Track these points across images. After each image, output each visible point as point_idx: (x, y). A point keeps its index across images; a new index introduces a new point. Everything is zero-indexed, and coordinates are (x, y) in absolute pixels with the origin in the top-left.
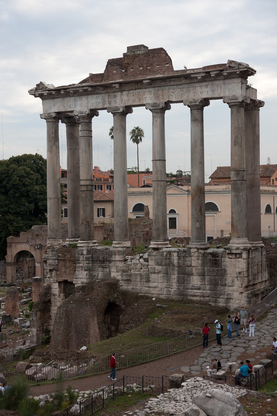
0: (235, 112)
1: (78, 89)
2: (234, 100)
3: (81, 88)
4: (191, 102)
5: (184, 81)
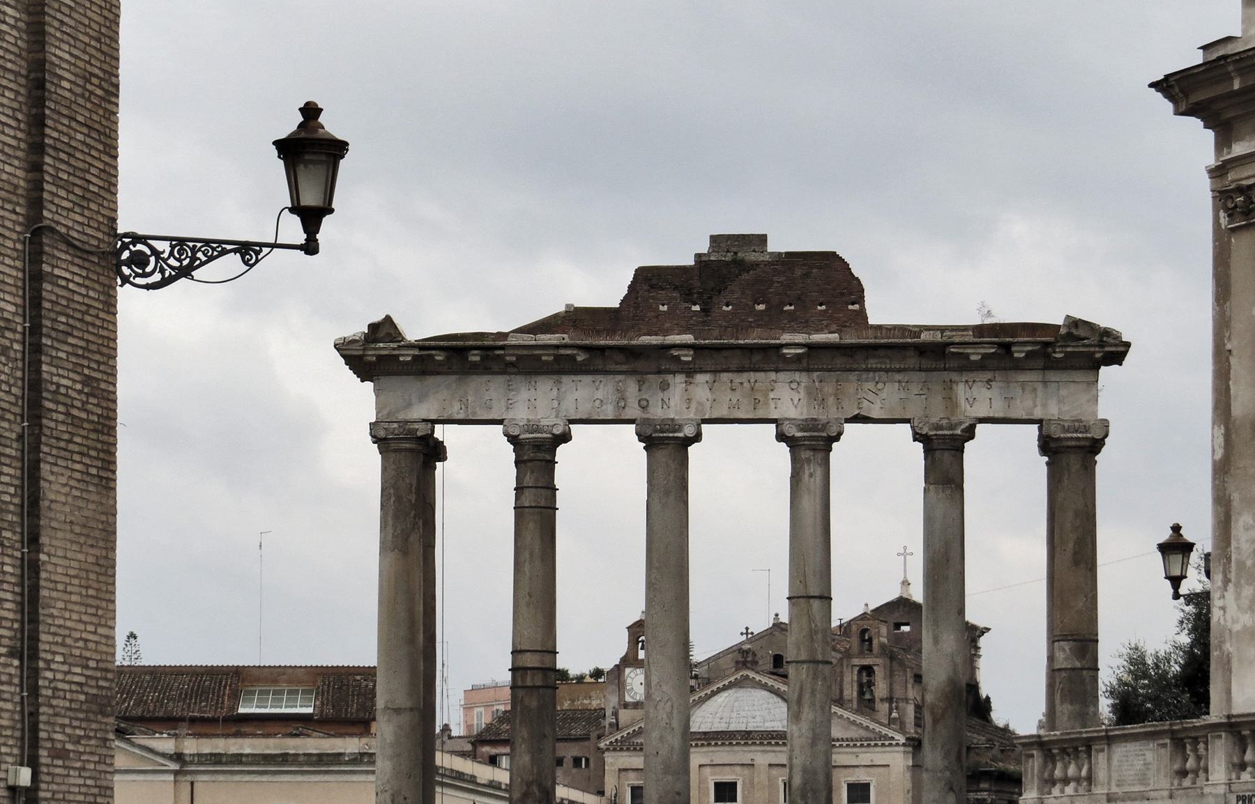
0: (1078, 466)
1: (538, 352)
2: (1076, 431)
3: (552, 352)
4: (938, 427)
5: (912, 361)
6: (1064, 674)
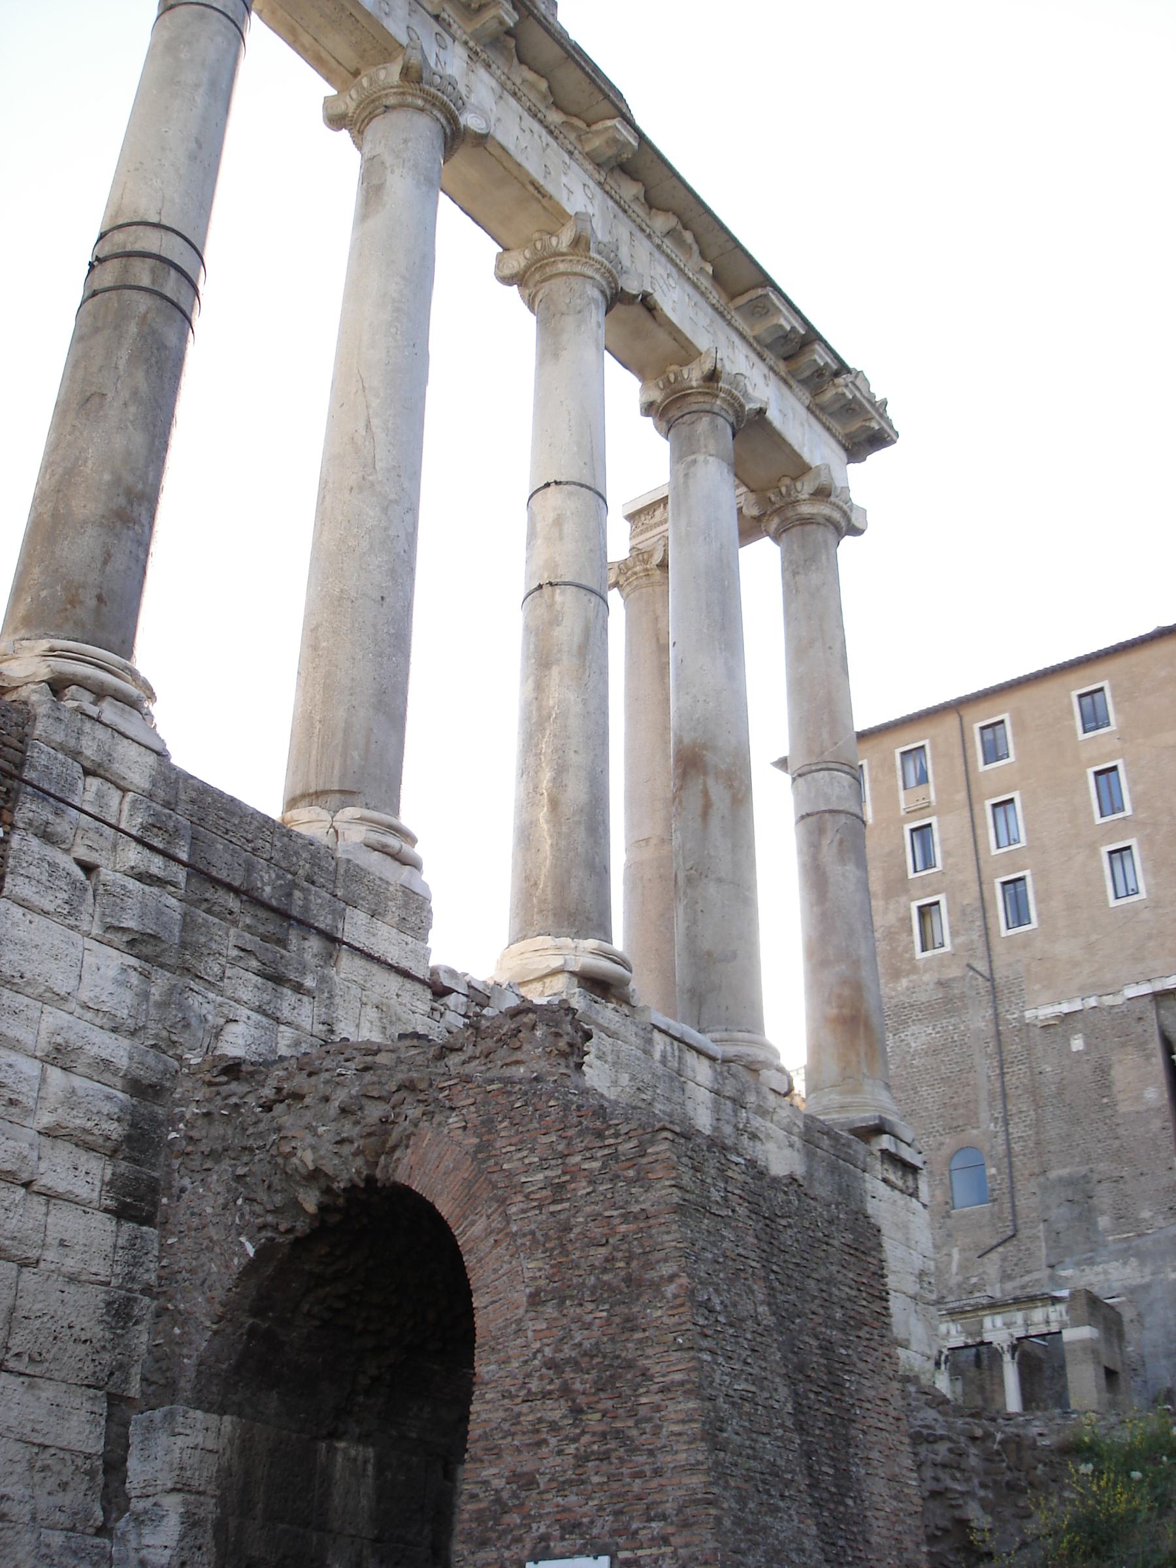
5: (705, 283)
6: (843, 819)
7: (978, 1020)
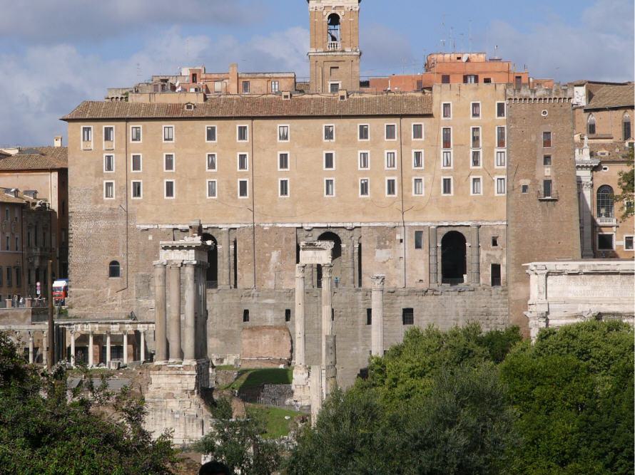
7: (121, 223)
